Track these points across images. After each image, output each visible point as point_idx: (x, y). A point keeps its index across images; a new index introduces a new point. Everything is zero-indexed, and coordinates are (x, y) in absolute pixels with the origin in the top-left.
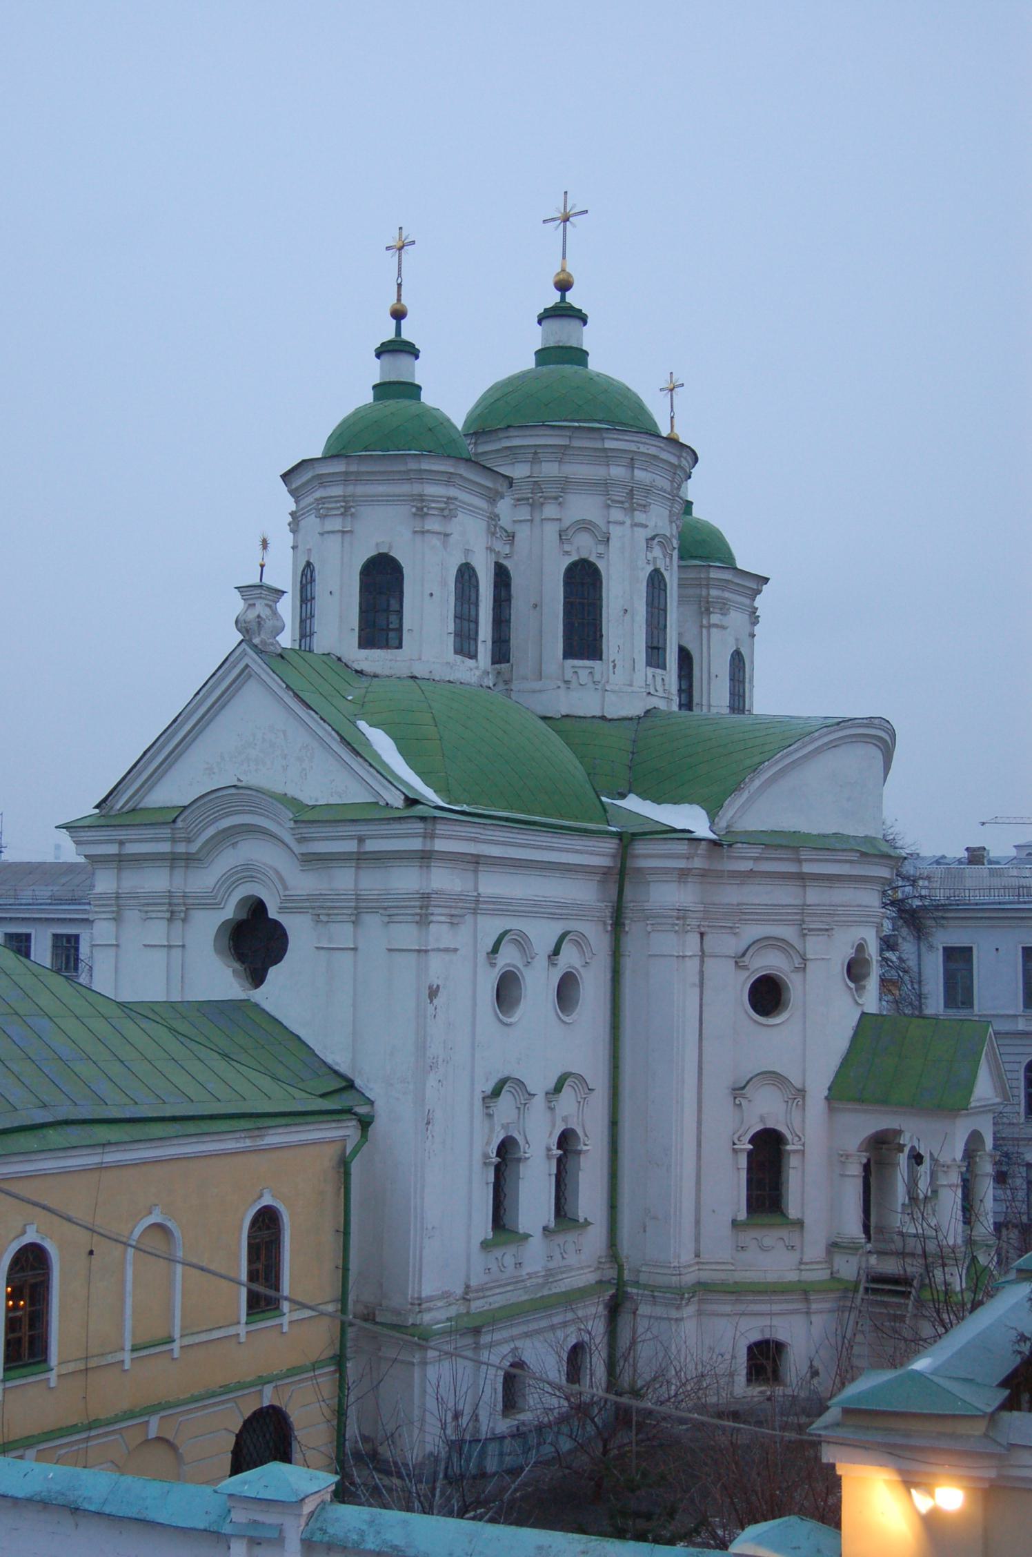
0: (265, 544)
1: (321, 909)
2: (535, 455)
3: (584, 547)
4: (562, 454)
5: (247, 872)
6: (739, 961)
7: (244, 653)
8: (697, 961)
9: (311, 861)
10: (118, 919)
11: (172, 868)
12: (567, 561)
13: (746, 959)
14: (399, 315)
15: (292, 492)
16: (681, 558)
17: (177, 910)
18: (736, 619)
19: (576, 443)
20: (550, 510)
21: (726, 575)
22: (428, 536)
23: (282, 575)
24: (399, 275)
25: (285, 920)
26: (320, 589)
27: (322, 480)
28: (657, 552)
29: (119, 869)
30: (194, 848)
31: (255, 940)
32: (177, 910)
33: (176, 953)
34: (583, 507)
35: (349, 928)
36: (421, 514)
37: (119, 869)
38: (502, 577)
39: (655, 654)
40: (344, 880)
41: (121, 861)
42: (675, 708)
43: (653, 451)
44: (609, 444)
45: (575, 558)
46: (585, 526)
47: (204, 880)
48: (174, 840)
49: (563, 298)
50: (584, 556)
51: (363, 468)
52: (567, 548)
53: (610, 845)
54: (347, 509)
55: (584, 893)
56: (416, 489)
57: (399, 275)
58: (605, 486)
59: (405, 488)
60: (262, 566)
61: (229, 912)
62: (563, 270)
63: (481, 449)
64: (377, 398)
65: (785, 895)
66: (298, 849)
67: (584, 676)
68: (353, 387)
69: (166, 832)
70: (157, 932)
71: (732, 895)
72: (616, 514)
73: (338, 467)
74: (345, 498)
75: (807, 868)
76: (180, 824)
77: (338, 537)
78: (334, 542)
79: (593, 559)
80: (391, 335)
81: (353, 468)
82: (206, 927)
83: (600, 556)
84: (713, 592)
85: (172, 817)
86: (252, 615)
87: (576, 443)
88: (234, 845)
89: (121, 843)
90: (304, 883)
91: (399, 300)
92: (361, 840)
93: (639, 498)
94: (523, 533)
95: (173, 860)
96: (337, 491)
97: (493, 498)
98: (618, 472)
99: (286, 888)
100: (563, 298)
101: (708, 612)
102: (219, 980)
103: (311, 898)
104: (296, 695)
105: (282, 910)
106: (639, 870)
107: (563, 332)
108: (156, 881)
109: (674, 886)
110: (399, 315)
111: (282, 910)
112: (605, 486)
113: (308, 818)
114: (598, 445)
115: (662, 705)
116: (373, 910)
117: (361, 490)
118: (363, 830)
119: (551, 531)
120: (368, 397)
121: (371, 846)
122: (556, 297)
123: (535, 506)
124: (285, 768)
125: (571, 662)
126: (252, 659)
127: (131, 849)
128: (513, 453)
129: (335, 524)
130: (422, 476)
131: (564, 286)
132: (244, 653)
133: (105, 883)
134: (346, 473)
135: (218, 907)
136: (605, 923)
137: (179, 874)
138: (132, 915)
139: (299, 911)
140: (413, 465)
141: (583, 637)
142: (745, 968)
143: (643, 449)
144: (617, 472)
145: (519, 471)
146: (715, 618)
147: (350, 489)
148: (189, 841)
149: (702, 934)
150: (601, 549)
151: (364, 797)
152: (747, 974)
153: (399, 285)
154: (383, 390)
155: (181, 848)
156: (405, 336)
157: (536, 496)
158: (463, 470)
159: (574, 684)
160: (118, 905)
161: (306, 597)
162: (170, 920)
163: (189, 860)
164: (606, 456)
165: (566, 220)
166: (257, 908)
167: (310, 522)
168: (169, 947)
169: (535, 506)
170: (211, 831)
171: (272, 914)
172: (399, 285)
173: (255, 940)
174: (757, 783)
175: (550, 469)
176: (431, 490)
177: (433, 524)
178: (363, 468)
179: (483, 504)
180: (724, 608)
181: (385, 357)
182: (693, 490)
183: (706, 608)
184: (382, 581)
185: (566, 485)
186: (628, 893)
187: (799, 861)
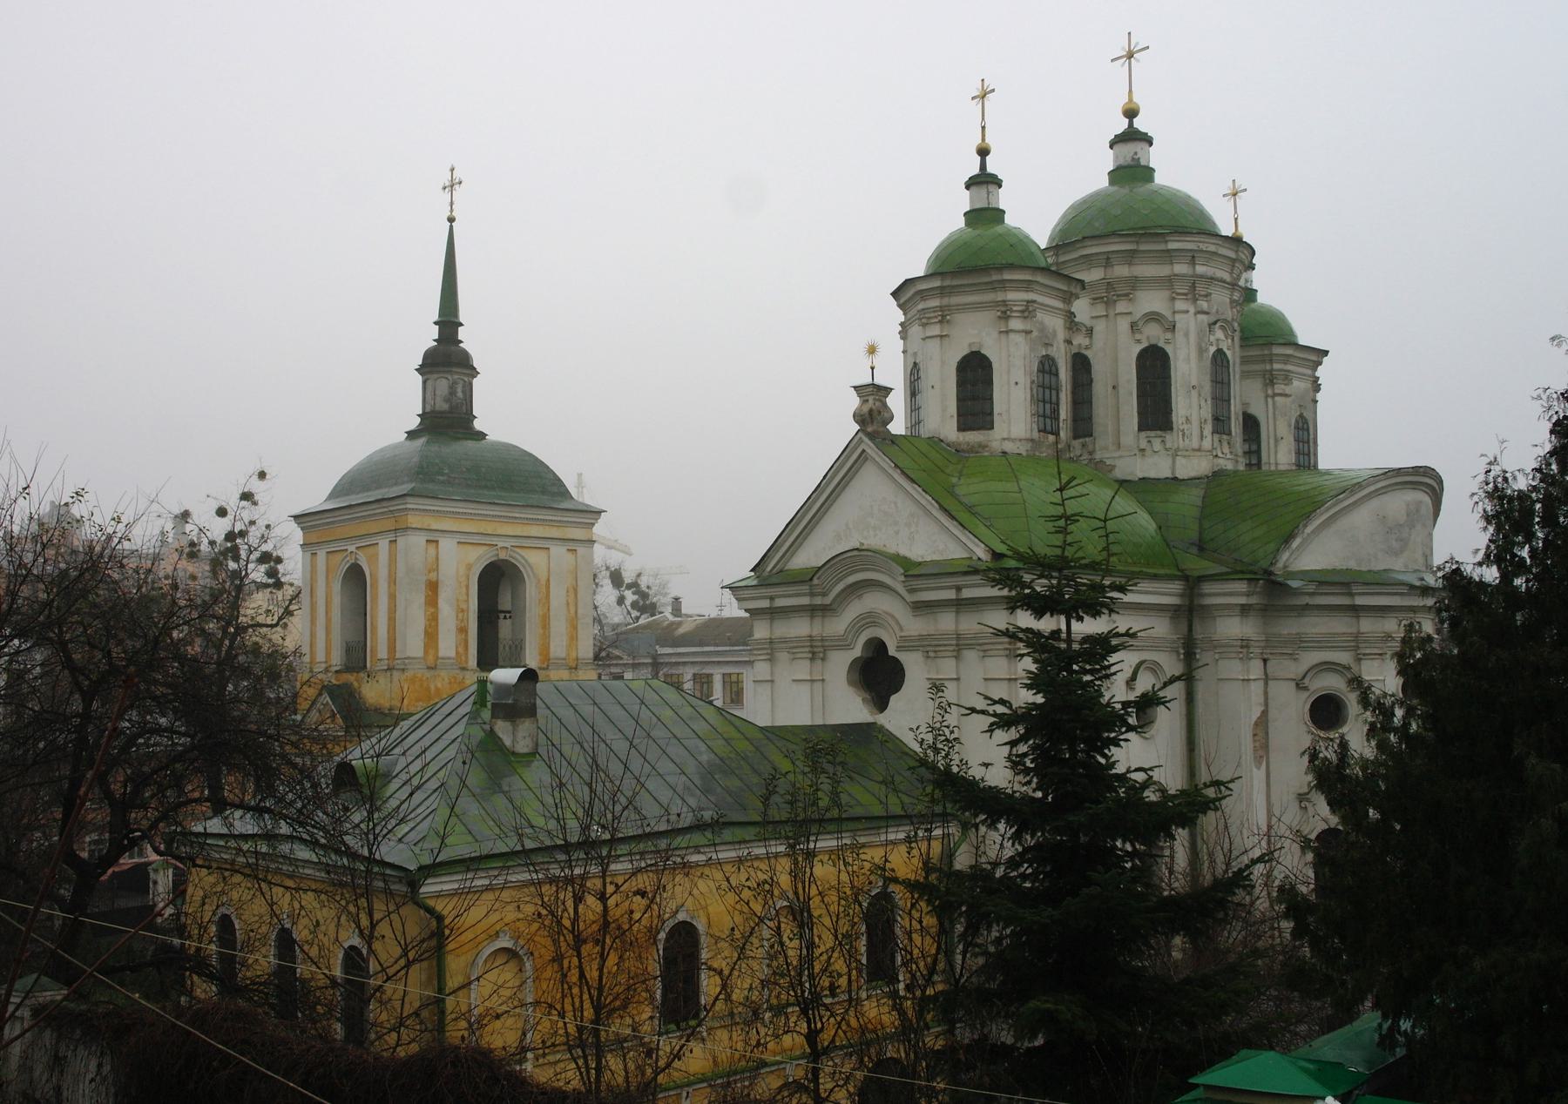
1: (930, 647)
2: (1107, 261)
3: (1153, 334)
4: (1130, 257)
5: (870, 619)
6: (1300, 686)
7: (861, 441)
8: (1261, 683)
9: (920, 608)
10: (771, 659)
11: (812, 617)
12: (1138, 348)
13: (1306, 681)
14: (983, 152)
15: (900, 306)
16: (1242, 339)
17: (817, 650)
18: (1298, 385)
19: (1142, 247)
20: (1121, 307)
21: (1289, 351)
22: (1012, 336)
23: (892, 374)
25: (903, 657)
26: (924, 384)
27: (923, 295)
28: (1219, 334)
29: (772, 620)
30: (828, 600)
31: (879, 674)
32: (817, 650)
33: (818, 686)
34: (1151, 301)
35: (952, 662)
36: (1005, 317)
37: (772, 620)
38: (1081, 364)
39: (1220, 424)
40: (946, 622)
41: (773, 613)
42: (1241, 467)
43: (1212, 248)
44: (1172, 246)
45: (1145, 344)
46: (1153, 317)
47: (838, 626)
48: (812, 595)
49: (1131, 124)
50: (1153, 342)
51: (955, 282)
52: (1138, 336)
53: (1177, 586)
54: (943, 316)
55: (1161, 628)
56: (1000, 296)
58: (1169, 282)
59: (989, 297)
61: (857, 652)
62: (1131, 100)
63: (1062, 259)
64: (968, 224)
65: (1339, 625)
66: (910, 598)
67: (1157, 445)
68: (947, 216)
69: (805, 588)
70: (803, 669)
71: (1289, 627)
72: (1180, 305)
73: (937, 283)
74: (941, 308)
75: (1359, 601)
76: (815, 581)
77: (938, 340)
78: (934, 346)
79: (1161, 344)
80: (976, 171)
81: (947, 283)
82: (840, 663)
83: (1167, 342)
84: (1276, 366)
85: (807, 578)
86: (866, 409)
87: (1142, 247)
88: (860, 597)
89: (772, 599)
90: (915, 626)
92: (959, 589)
93: (1200, 289)
94: (1100, 327)
95: (813, 611)
96: (935, 303)
97: (1068, 298)
98: (1181, 268)
99: (901, 629)
100: (1131, 124)
101: (1272, 383)
102: (850, 708)
103: (921, 637)
104: (903, 473)
105: (899, 648)
106: (1203, 607)
107: (1128, 150)
108: (800, 628)
109: (1237, 620)
110: (983, 152)
111: (899, 648)
112: (1169, 282)
113: (913, 572)
114: (1162, 247)
115: (1230, 466)
116: (970, 647)
117: (955, 300)
119: (1123, 325)
120: (960, 223)
122: (1122, 125)
123: (1109, 303)
124: (897, 533)
125: (1143, 434)
126: (868, 446)
127: (780, 603)
128: (1088, 261)
129: (935, 330)
130: (1003, 285)
131: (1131, 113)
132: (861, 441)
133: (761, 631)
134: (942, 288)
135: (849, 647)
136: (1178, 653)
137: (818, 621)
138: (783, 656)
140: (995, 277)
141: (1155, 411)
142: (1306, 689)
143: (1203, 247)
144: (1181, 268)
145: (1092, 275)
146: (1279, 388)
147: (946, 301)
148: (824, 595)
149: (1265, 661)
150: (1169, 335)
151: (959, 554)
152: (1306, 694)
154: (973, 217)
155: (818, 601)
156: (990, 169)
157: (1109, 294)
158: (1040, 278)
159: (1148, 452)
160: (771, 649)
161: (913, 392)
162: (812, 659)
164: (1169, 256)
165: (1130, 55)
166: (877, 647)
167: (915, 330)
168: (812, 681)
169: (1109, 303)
171: (892, 652)
173: (879, 674)
174: (1309, 530)
175: (1121, 271)
176: (1011, 296)
177: (1016, 324)
178: (955, 282)
179: (1060, 305)
180: (1287, 379)
181: (973, 188)
182: (1259, 279)
183: (1270, 380)
184: (975, 375)
185: (1135, 283)
186: (1197, 627)
187: (1351, 595)
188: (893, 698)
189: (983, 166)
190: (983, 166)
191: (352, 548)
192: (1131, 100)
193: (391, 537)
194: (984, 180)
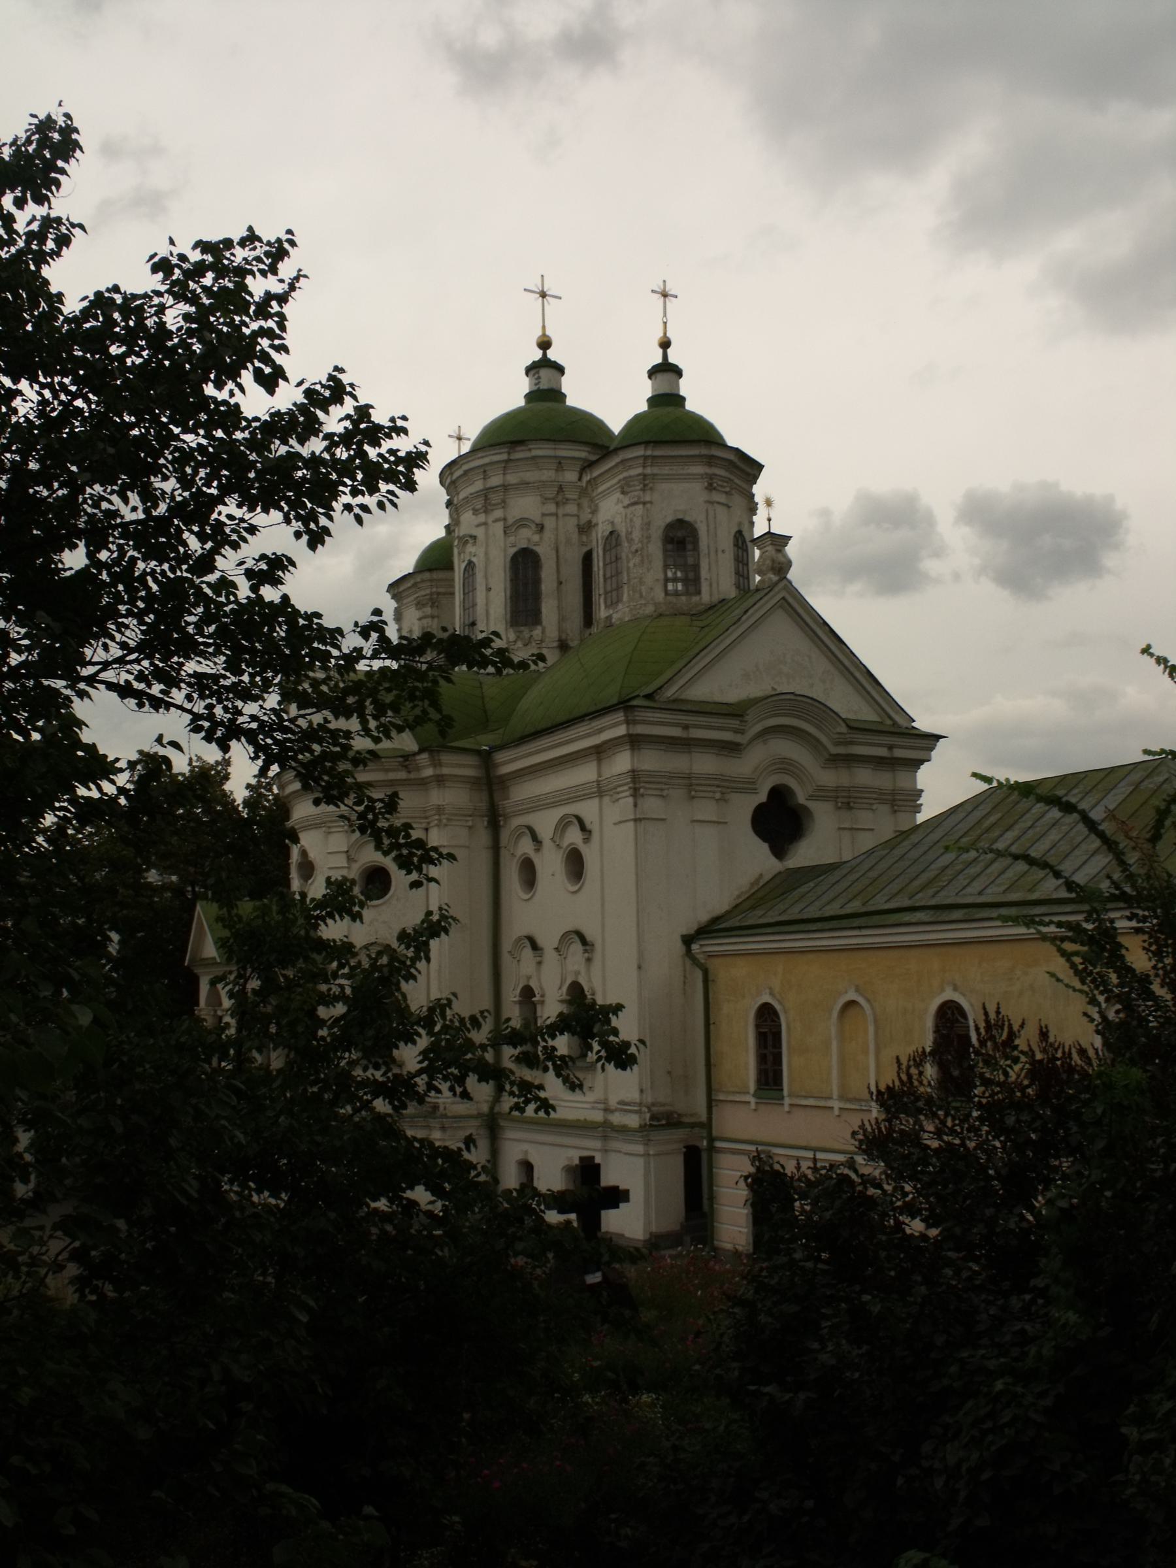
5: (785, 765)
14: (665, 344)
17: (725, 787)
24: (665, 315)
25: (812, 805)
40: (865, 777)
49: (545, 354)
57: (665, 315)
60: (769, 520)
61: (762, 797)
62: (544, 335)
69: (734, 723)
80: (659, 360)
82: (744, 807)
85: (736, 712)
90: (829, 778)
91: (665, 333)
92: (891, 748)
96: (722, 472)
100: (545, 354)
103: (837, 789)
105: (811, 797)
108: (705, 764)
110: (665, 344)
121: (899, 753)
122: (537, 355)
129: (722, 498)
131: (545, 344)
135: (754, 791)
139: (824, 799)
148: (742, 732)
153: (665, 323)
155: (738, 738)
163: (732, 749)
170: (758, 728)
172: (665, 323)
188: (765, 846)
192: (544, 335)
194: (666, 370)
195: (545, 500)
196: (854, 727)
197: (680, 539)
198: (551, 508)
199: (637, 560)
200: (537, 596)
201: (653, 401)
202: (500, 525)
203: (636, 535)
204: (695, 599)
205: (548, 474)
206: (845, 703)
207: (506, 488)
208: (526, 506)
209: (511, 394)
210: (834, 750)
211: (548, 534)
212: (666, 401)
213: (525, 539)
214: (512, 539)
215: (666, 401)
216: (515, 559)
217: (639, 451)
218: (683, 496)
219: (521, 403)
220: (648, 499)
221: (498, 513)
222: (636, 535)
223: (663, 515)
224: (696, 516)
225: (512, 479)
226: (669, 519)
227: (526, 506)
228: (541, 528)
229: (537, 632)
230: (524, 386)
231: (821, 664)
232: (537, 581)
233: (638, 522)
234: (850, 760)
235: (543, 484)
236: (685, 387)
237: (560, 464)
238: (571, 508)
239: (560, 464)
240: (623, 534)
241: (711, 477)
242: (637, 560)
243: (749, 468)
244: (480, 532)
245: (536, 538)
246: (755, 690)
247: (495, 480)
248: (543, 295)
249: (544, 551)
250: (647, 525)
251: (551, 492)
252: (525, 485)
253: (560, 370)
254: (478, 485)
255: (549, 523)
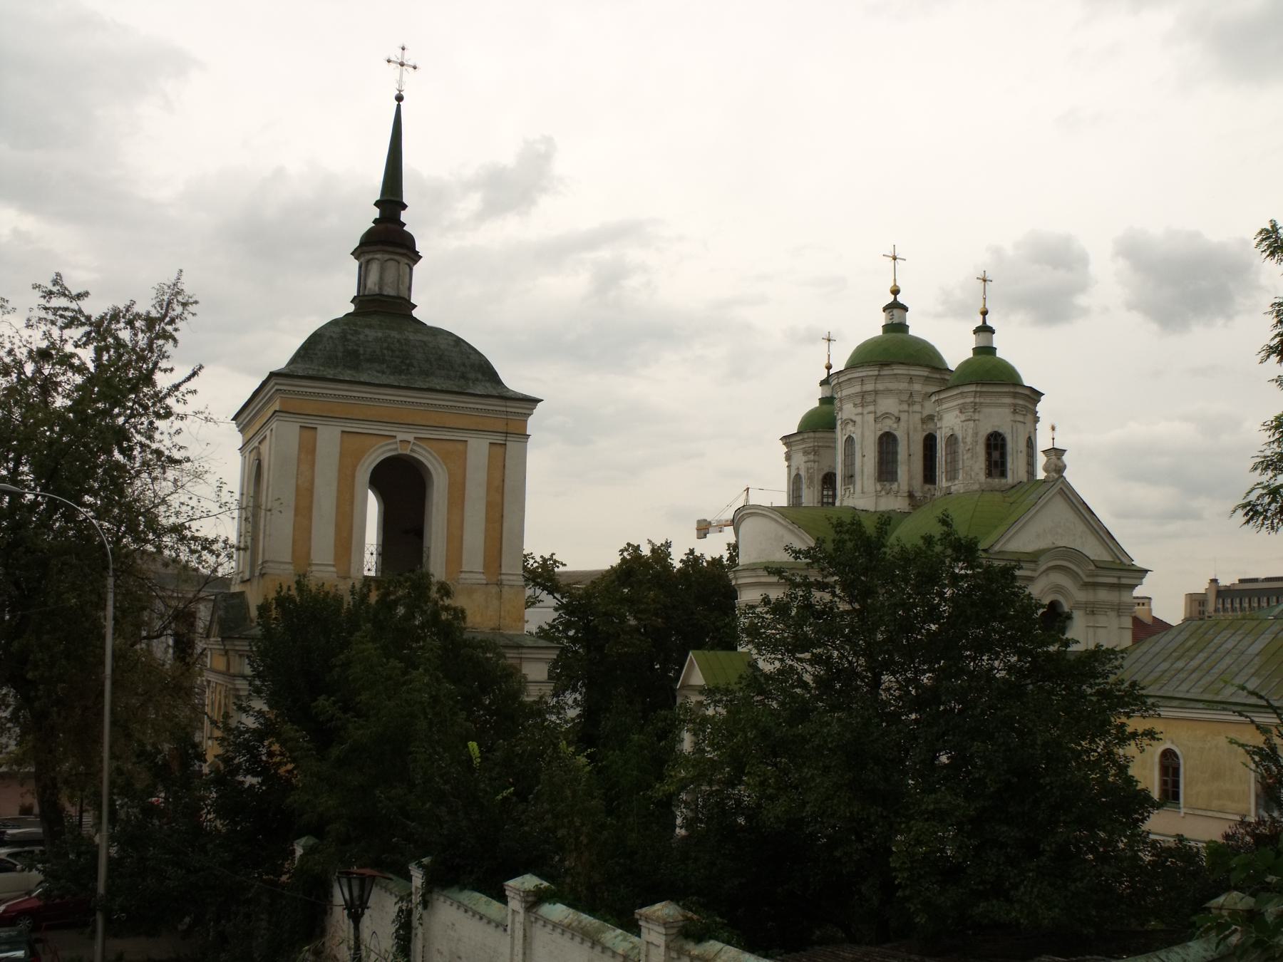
0: (1053, 429)
5: (1059, 589)
9: (1086, 585)
40: (1103, 595)
69: (1032, 566)
80: (980, 323)
90: (1081, 596)
92: (1119, 578)
96: (1021, 402)
118: (1119, 574)
121: (1124, 581)
131: (895, 292)
148: (1034, 570)
156: (989, 323)
170: (1044, 567)
189: (984, 321)
190: (984, 321)
191: (410, 437)
193: (499, 439)
195: (902, 402)
196: (1100, 566)
197: (996, 444)
198: (905, 407)
199: (969, 455)
200: (895, 462)
201: (977, 351)
202: (872, 416)
203: (969, 440)
204: (1003, 481)
205: (903, 385)
206: (1094, 550)
207: (876, 392)
208: (889, 404)
209: (872, 326)
210: (1087, 580)
211: (902, 424)
212: (984, 351)
213: (888, 425)
214: (879, 426)
215: (984, 351)
216: (881, 438)
217: (973, 388)
218: (997, 417)
219: (879, 332)
220: (976, 417)
221: (871, 408)
222: (969, 440)
223: (986, 429)
224: (1005, 430)
225: (880, 387)
226: (990, 431)
227: (889, 404)
228: (898, 419)
229: (895, 486)
230: (882, 319)
231: (1081, 527)
232: (895, 453)
233: (970, 432)
234: (1095, 585)
235: (901, 392)
236: (997, 341)
237: (911, 379)
238: (917, 408)
239: (911, 379)
240: (960, 438)
241: (1015, 405)
242: (969, 455)
243: (1035, 395)
244: (858, 419)
245: (895, 426)
246: (1042, 544)
247: (869, 387)
248: (895, 258)
249: (900, 434)
250: (976, 434)
251: (905, 397)
252: (889, 391)
253: (905, 309)
254: (857, 389)
255: (904, 417)
